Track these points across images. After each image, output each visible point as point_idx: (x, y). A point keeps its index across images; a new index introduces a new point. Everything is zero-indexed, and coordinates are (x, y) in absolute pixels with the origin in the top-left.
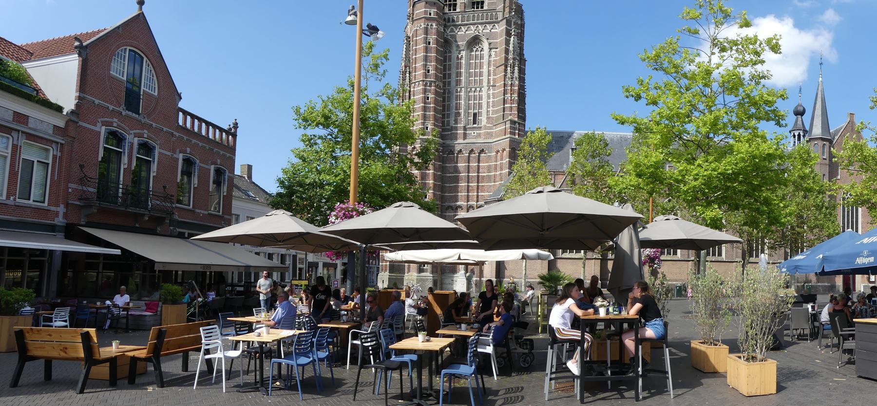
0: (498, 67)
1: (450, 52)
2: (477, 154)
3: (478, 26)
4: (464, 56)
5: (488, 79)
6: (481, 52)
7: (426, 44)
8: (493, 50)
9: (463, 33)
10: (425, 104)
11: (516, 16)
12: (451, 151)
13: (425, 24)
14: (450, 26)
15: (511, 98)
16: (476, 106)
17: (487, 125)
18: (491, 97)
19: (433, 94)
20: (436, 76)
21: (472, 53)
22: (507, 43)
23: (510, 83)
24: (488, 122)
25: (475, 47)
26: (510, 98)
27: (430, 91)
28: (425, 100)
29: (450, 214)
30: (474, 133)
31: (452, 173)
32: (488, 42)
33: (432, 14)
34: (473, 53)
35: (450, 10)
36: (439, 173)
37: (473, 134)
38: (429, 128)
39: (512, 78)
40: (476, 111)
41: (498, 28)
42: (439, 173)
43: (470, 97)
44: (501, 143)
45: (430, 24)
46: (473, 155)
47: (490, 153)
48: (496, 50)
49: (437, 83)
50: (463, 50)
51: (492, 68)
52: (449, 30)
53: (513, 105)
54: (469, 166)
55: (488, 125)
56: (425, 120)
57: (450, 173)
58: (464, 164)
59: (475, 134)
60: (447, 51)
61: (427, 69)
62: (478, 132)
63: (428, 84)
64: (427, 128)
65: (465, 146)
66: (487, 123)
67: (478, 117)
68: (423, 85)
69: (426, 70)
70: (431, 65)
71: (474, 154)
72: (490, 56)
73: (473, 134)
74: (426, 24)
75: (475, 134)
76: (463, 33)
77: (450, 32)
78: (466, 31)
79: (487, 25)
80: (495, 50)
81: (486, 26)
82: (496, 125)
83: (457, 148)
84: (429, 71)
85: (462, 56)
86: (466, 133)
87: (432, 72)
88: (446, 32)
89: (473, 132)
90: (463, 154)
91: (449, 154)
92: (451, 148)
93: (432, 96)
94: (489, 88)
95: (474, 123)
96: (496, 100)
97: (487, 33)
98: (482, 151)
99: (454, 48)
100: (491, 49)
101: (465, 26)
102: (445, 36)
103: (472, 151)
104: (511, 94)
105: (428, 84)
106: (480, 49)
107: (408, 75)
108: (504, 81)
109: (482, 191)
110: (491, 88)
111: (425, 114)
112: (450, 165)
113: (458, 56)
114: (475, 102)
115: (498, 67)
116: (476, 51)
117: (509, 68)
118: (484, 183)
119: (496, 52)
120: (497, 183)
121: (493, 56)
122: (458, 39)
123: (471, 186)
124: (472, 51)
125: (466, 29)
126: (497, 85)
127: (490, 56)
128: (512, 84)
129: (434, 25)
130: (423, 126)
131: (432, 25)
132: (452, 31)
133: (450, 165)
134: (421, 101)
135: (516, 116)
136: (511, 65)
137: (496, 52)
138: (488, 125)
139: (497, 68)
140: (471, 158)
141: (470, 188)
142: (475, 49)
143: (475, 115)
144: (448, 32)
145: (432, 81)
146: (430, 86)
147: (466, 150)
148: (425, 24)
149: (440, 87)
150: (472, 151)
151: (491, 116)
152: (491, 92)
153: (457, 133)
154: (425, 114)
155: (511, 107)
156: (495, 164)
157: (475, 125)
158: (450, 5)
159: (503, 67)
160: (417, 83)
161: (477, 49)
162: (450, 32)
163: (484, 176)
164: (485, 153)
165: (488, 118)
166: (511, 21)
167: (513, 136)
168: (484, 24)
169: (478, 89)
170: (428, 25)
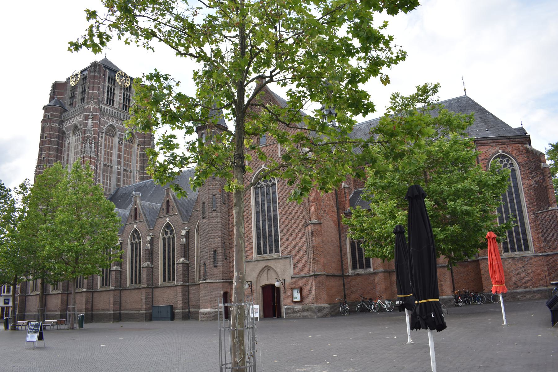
166: (90, 108)
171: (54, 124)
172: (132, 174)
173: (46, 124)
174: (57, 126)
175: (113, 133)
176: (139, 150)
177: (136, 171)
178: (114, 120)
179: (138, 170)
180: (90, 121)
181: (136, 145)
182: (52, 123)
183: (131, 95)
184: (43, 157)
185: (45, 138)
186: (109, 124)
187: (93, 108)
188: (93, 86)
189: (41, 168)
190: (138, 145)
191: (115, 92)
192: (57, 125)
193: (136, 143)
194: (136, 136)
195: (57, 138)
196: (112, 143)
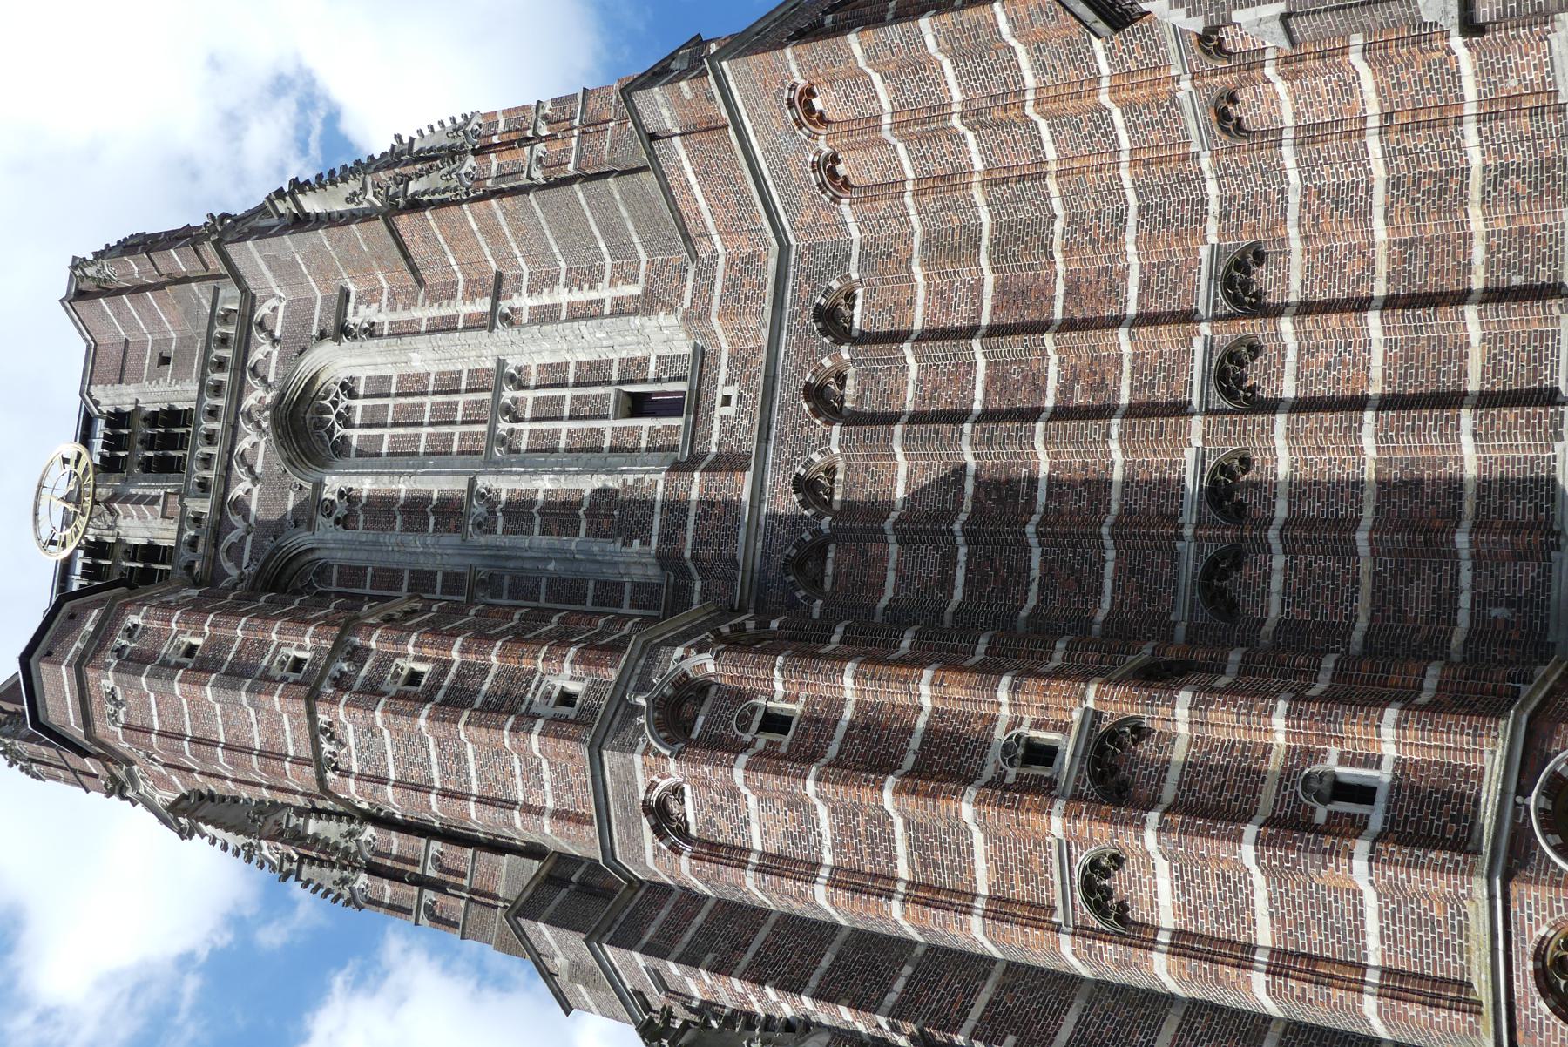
0: (414, 269)
1: (323, 571)
2: (845, 352)
3: (249, 415)
5: (465, 329)
8: (351, 319)
9: (256, 492)
10: (427, 700)
12: (797, 565)
14: (214, 560)
17: (687, 304)
19: (404, 642)
21: (354, 443)
23: (471, 161)
25: (331, 432)
26: (541, 147)
27: (385, 660)
29: (1276, 583)
31: (949, 561)
34: (355, 435)
37: (730, 411)
38: (573, 687)
41: (273, 302)
43: (541, 443)
44: (766, 151)
45: (121, 640)
46: (850, 389)
47: (848, 256)
48: (352, 298)
50: (318, 486)
51: (424, 313)
54: (917, 418)
55: (688, 295)
57: (947, 582)
58: (898, 450)
59: (732, 391)
62: (722, 378)
63: (345, 667)
64: (567, 699)
65: (779, 453)
66: (673, 311)
67: (645, 381)
68: (334, 701)
71: (841, 379)
73: (730, 411)
75: (732, 391)
76: (256, 492)
77: (238, 565)
78: (251, 470)
79: (250, 363)
81: (254, 370)
82: (687, 238)
83: (783, 501)
86: (719, 455)
89: (721, 411)
90: (831, 471)
91: (817, 583)
92: (777, 559)
94: (505, 317)
96: (563, 264)
97: (281, 358)
98: (832, 321)
99: (303, 538)
100: (343, 331)
101: (233, 481)
103: (823, 400)
105: (345, 667)
107: (313, 826)
108: (459, 203)
109: (1115, 290)
110: (504, 306)
112: (891, 576)
114: (566, 413)
115: (414, 269)
116: (348, 424)
118: (1050, 282)
119: (359, 301)
120: (1051, 152)
122: (275, 517)
123: (1064, 390)
124: (341, 448)
126: (494, 267)
128: (475, 153)
130: (540, 723)
131: (130, 632)
133: (891, 576)
137: (359, 301)
138: (688, 295)
139: (420, 282)
140: (867, 408)
141: (1080, 399)
142: (340, 431)
146: (358, 655)
147: (802, 441)
150: (823, 400)
152: (523, 302)
153: (700, 503)
156: (916, 193)
159: (404, 222)
160: (327, 747)
161: (339, 416)
163: (1002, 290)
164: (850, 297)
165: (648, 304)
168: (243, 378)
169: (508, 395)
170: (119, 651)
173: (121, 640)
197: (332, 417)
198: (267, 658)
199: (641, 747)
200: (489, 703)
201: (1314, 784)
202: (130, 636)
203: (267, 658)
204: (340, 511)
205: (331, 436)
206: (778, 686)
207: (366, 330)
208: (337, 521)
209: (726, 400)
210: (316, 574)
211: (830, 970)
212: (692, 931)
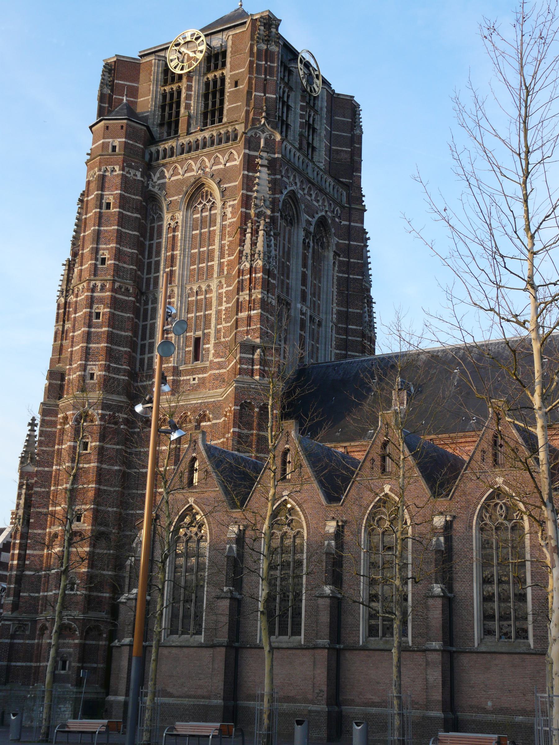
4: (180, 224)
6: (210, 210)
7: (101, 208)
9: (180, 177)
10: (90, 326)
11: (269, 127)
13: (123, 170)
14: (159, 166)
15: (250, 296)
16: (201, 321)
18: (224, 299)
20: (117, 270)
22: (248, 183)
24: (217, 355)
25: (201, 203)
28: (90, 320)
30: (194, 379)
32: (219, 187)
33: (117, 149)
35: (169, 134)
36: (116, 468)
39: (252, 255)
40: (199, 333)
42: (116, 468)
49: (117, 285)
52: (158, 175)
53: (253, 312)
56: (87, 360)
59: (197, 379)
60: (155, 217)
61: (100, 257)
64: (92, 375)
69: (96, 259)
70: (107, 249)
72: (224, 216)
74: (103, 168)
75: (196, 382)
80: (232, 203)
84: (103, 261)
85: (177, 223)
87: (110, 262)
88: (153, 180)
89: (191, 377)
93: (105, 310)
95: (196, 358)
98: (204, 417)
102: (150, 187)
104: (250, 290)
106: (209, 205)
111: (87, 348)
113: (170, 224)
117: (248, 236)
121: (229, 215)
125: (185, 167)
127: (224, 216)
129: (117, 168)
131: (113, 170)
132: (163, 176)
134: (83, 322)
135: (257, 335)
136: (252, 229)
137: (233, 206)
143: (197, 341)
144: (155, 179)
145: (106, 280)
148: (100, 170)
149: (127, 290)
151: (223, 340)
154: (87, 348)
155: (249, 317)
157: (199, 364)
158: (169, 124)
161: (205, 204)
162: (159, 179)
164: (209, 420)
166: (259, 138)
167: (247, 378)
171: (132, 172)
172: (322, 329)
173: (109, 168)
174: (139, 177)
175: (291, 213)
176: (336, 269)
177: (331, 324)
178: (297, 181)
179: (334, 320)
180: (263, 175)
181: (332, 254)
182: (127, 169)
183: (316, 117)
184: (100, 257)
185: (104, 206)
186: (289, 189)
187: (266, 139)
188: (266, 80)
189: (95, 286)
190: (336, 254)
191: (291, 103)
192: (139, 174)
193: (333, 248)
194: (333, 230)
195: (137, 211)
196: (289, 242)
197: (204, 202)
198: (104, 246)
199: (74, 412)
200: (90, 350)
201: (73, 579)
202: (112, 171)
203: (104, 246)
204: (173, 224)
205: (199, 204)
206: (94, 444)
207: (224, 213)
208: (170, 224)
209: (194, 379)
210: (160, 214)
211: (44, 471)
212: (50, 429)
